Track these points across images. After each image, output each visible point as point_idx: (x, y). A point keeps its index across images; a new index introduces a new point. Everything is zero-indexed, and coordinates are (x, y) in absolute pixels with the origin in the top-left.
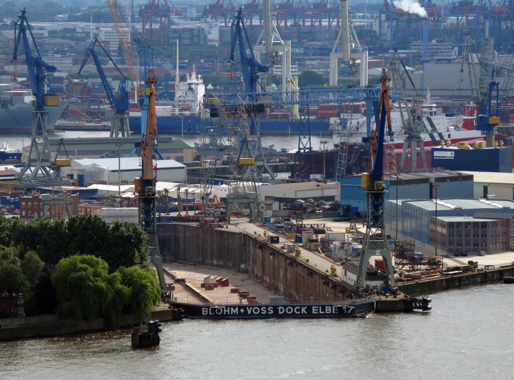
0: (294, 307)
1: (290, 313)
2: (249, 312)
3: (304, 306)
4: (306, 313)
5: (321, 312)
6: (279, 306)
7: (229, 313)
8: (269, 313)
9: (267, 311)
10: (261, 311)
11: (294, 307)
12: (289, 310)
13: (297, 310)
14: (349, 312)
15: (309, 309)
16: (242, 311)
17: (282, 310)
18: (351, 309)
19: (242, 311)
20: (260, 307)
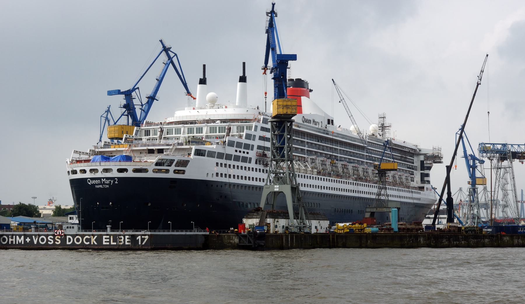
0: (83, 236)
1: (78, 243)
2: (35, 242)
3: (94, 235)
4: (96, 243)
5: (112, 243)
6: (65, 235)
7: (14, 243)
8: (56, 243)
9: (55, 241)
10: (48, 241)
11: (83, 236)
12: (78, 240)
13: (87, 240)
14: (143, 244)
15: (99, 239)
16: (28, 240)
17: (69, 241)
18: (146, 240)
19: (28, 240)
20: (47, 236)
